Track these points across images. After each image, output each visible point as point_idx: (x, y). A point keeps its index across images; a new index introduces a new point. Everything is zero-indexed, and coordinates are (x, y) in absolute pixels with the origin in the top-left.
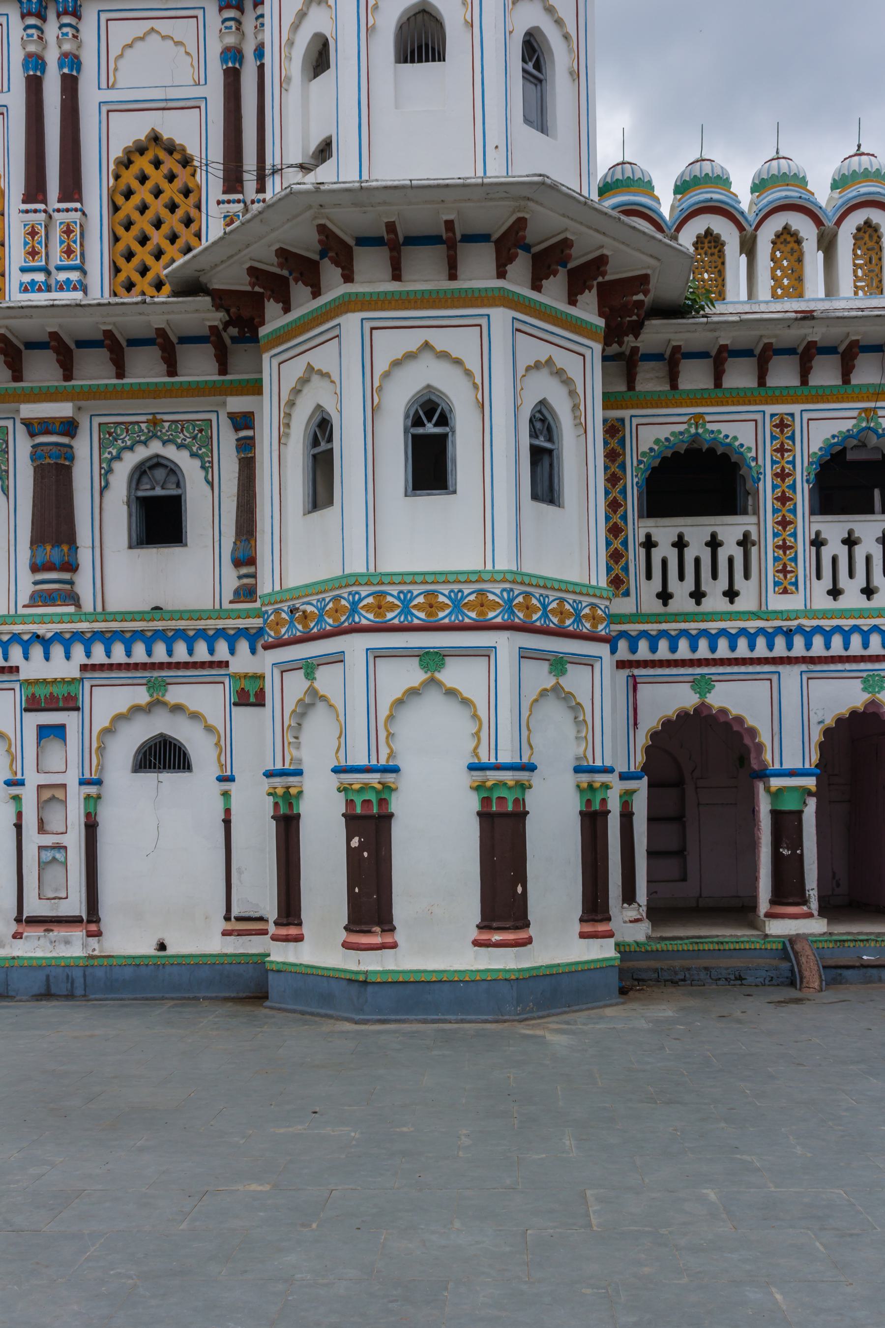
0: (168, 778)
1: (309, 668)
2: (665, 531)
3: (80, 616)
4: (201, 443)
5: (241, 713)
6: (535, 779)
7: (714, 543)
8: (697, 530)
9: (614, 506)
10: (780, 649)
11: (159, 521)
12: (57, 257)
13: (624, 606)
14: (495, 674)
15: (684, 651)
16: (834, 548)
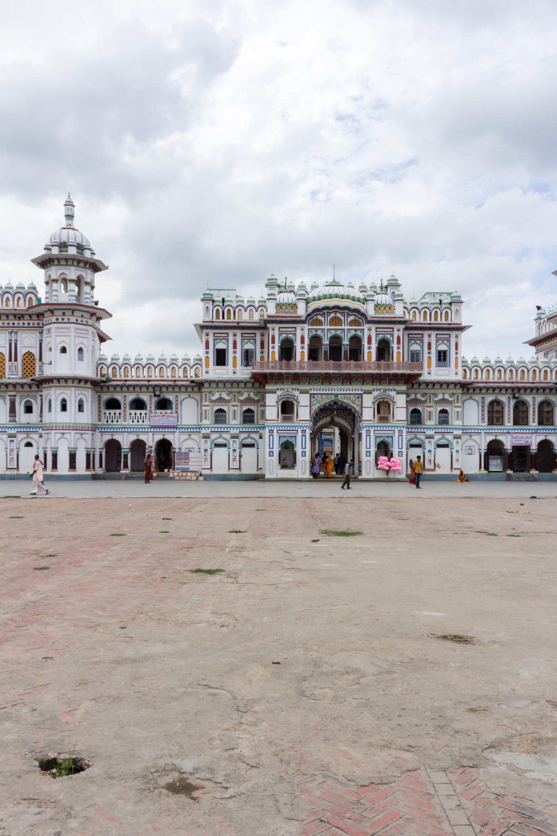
0: (30, 448)
1: (48, 434)
2: (108, 412)
3: (16, 424)
4: (35, 398)
5: (40, 439)
6: (78, 450)
7: (115, 414)
8: (113, 412)
9: (99, 408)
10: (123, 430)
11: (29, 409)
12: (13, 370)
13: (100, 423)
14: (71, 436)
15: (109, 430)
16: (133, 415)
